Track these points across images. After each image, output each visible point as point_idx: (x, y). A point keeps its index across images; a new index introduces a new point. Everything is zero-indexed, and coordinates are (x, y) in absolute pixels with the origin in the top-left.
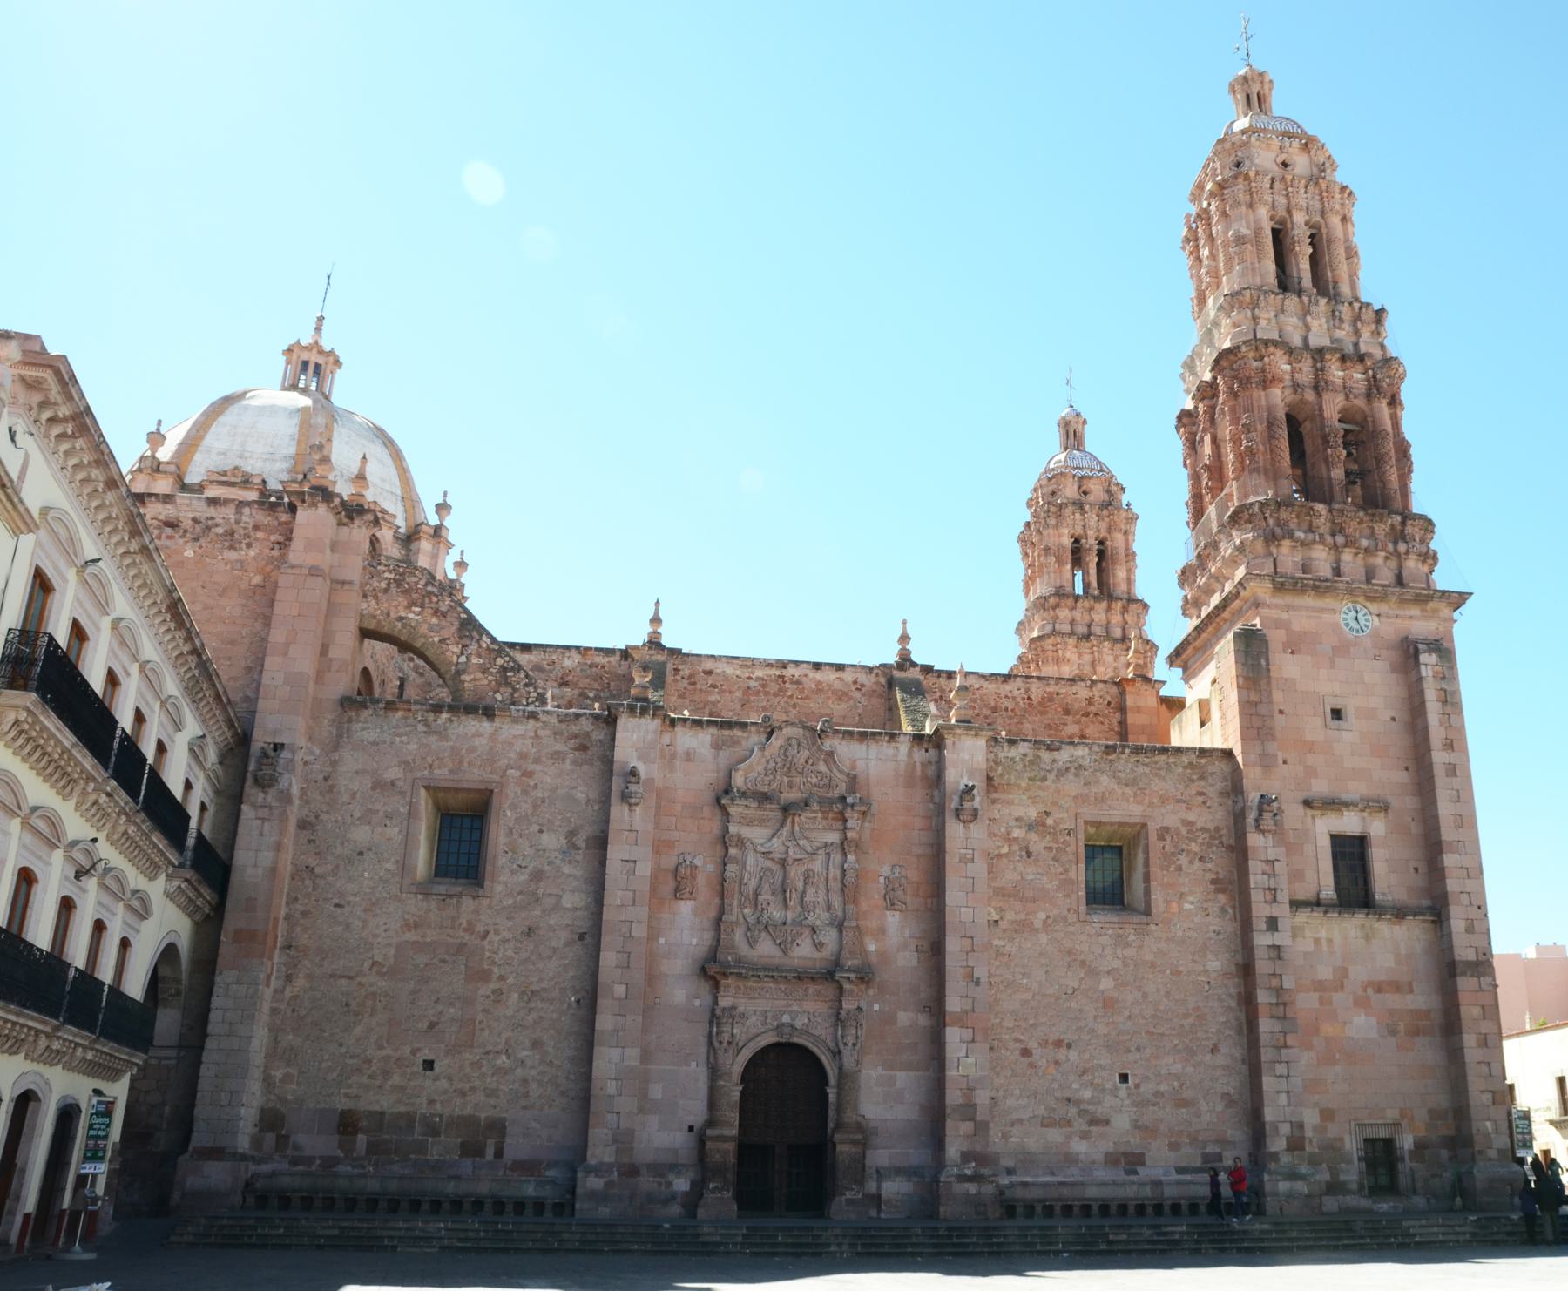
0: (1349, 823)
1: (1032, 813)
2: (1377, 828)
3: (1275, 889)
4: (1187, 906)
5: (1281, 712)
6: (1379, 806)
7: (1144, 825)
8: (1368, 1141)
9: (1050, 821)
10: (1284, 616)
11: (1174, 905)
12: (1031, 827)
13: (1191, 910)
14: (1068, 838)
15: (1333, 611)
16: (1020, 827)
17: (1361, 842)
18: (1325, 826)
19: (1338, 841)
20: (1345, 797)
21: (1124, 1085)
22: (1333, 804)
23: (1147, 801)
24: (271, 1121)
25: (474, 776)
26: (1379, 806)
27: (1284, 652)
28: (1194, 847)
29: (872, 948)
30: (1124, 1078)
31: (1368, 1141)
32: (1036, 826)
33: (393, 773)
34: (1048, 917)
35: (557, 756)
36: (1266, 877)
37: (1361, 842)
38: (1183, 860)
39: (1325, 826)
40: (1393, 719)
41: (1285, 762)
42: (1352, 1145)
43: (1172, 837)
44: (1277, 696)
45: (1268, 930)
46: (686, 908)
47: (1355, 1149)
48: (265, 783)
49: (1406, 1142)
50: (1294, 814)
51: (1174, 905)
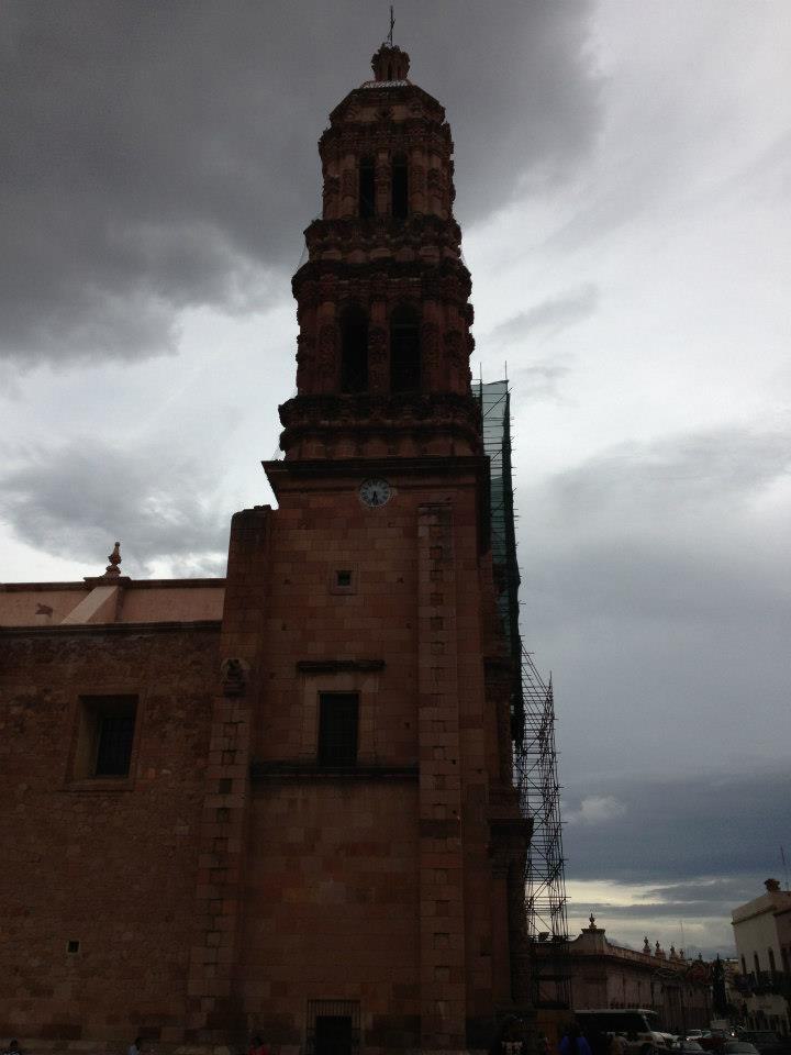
0: (342, 683)
1: (33, 691)
3: (235, 751)
4: (164, 771)
5: (287, 582)
6: (375, 667)
7: (137, 696)
8: (319, 1019)
9: (48, 698)
10: (303, 497)
11: (152, 772)
13: (167, 775)
14: (60, 712)
15: (352, 489)
16: (19, 705)
17: (352, 699)
18: (312, 688)
19: (326, 699)
20: (340, 658)
21: (74, 954)
23: (143, 673)
27: (299, 528)
28: (181, 714)
30: (74, 946)
31: (319, 1019)
34: (30, 788)
36: (226, 740)
37: (352, 699)
39: (312, 688)
40: (401, 580)
41: (284, 628)
42: (302, 1022)
43: (161, 707)
45: (220, 793)
47: (305, 1027)
49: (365, 1021)
51: (152, 772)
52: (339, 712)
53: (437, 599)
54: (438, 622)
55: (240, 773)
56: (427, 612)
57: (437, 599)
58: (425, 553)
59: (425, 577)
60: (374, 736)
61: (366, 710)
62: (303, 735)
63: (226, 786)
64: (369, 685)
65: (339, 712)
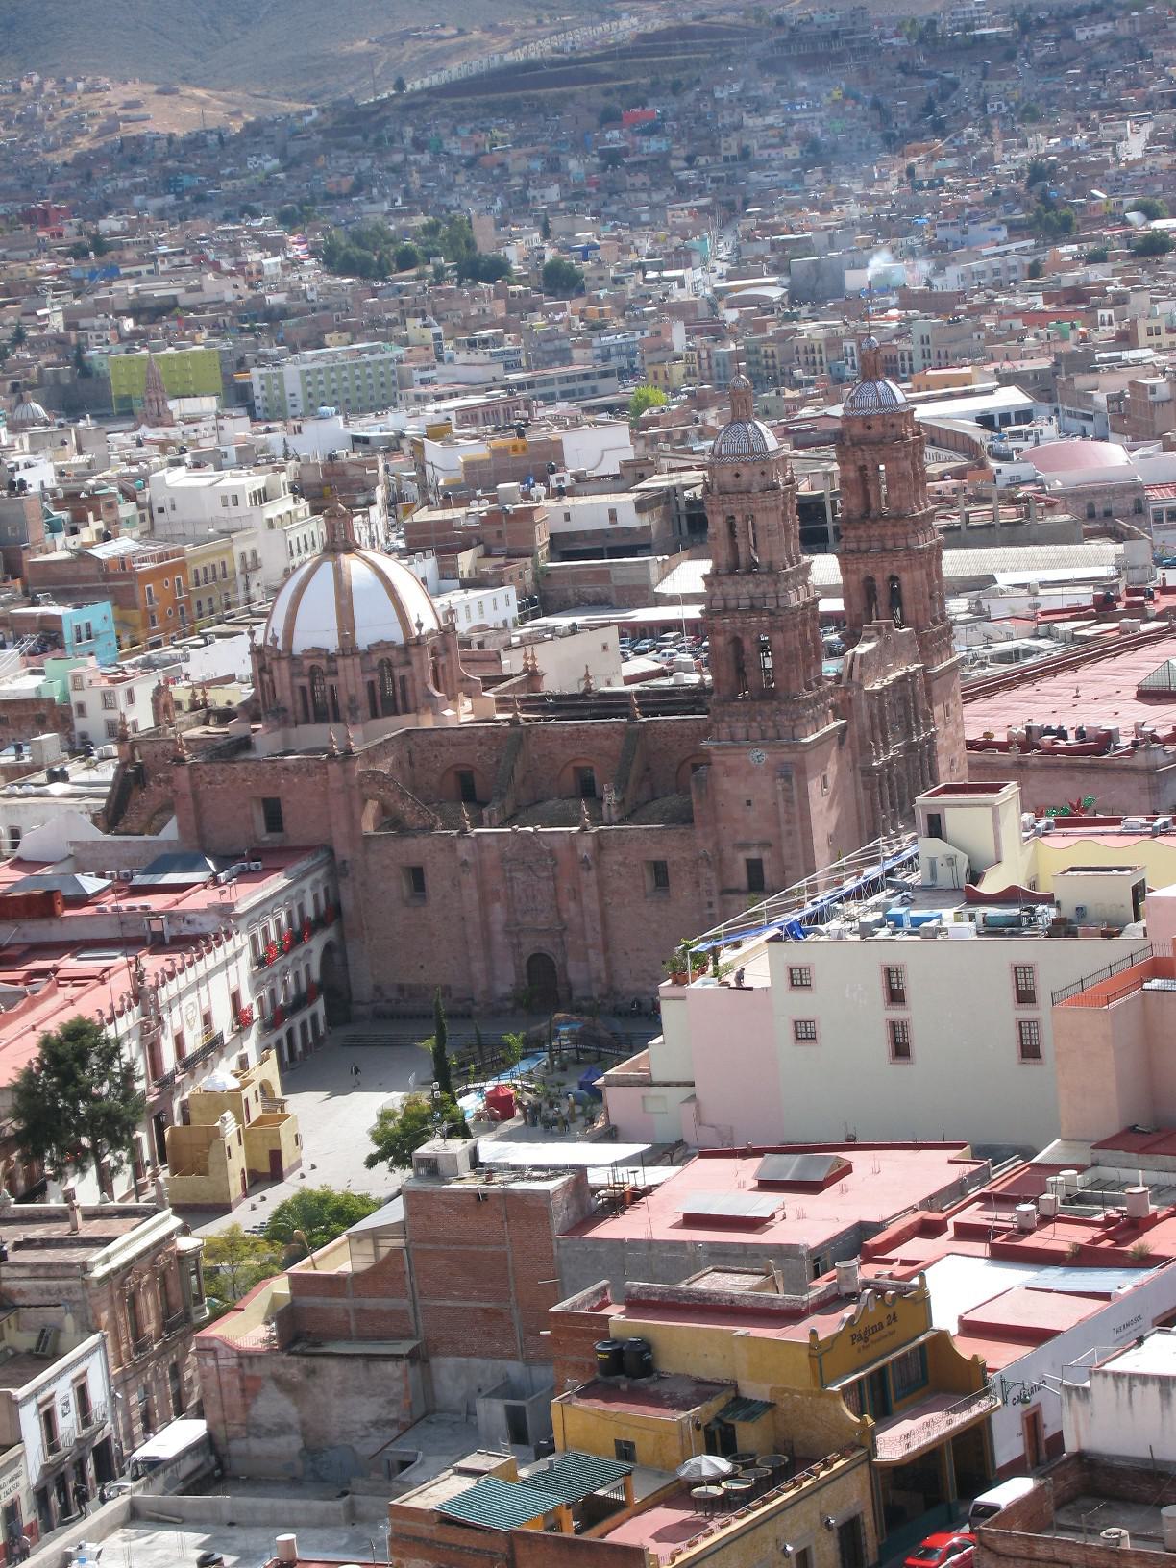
0: (754, 854)
1: (620, 858)
2: (766, 855)
6: (765, 845)
12: (623, 864)
22: (745, 846)
24: (377, 988)
25: (415, 861)
26: (765, 845)
29: (565, 916)
32: (623, 864)
33: (388, 861)
35: (442, 850)
38: (682, 874)
39: (741, 857)
44: (720, 798)
46: (497, 906)
48: (346, 876)
50: (728, 852)
52: (755, 867)
53: (788, 822)
54: (789, 833)
55: (715, 899)
56: (784, 828)
57: (788, 822)
58: (781, 799)
59: (782, 810)
60: (769, 874)
61: (765, 866)
62: (741, 878)
63: (710, 905)
64: (766, 855)
65: (755, 867)
